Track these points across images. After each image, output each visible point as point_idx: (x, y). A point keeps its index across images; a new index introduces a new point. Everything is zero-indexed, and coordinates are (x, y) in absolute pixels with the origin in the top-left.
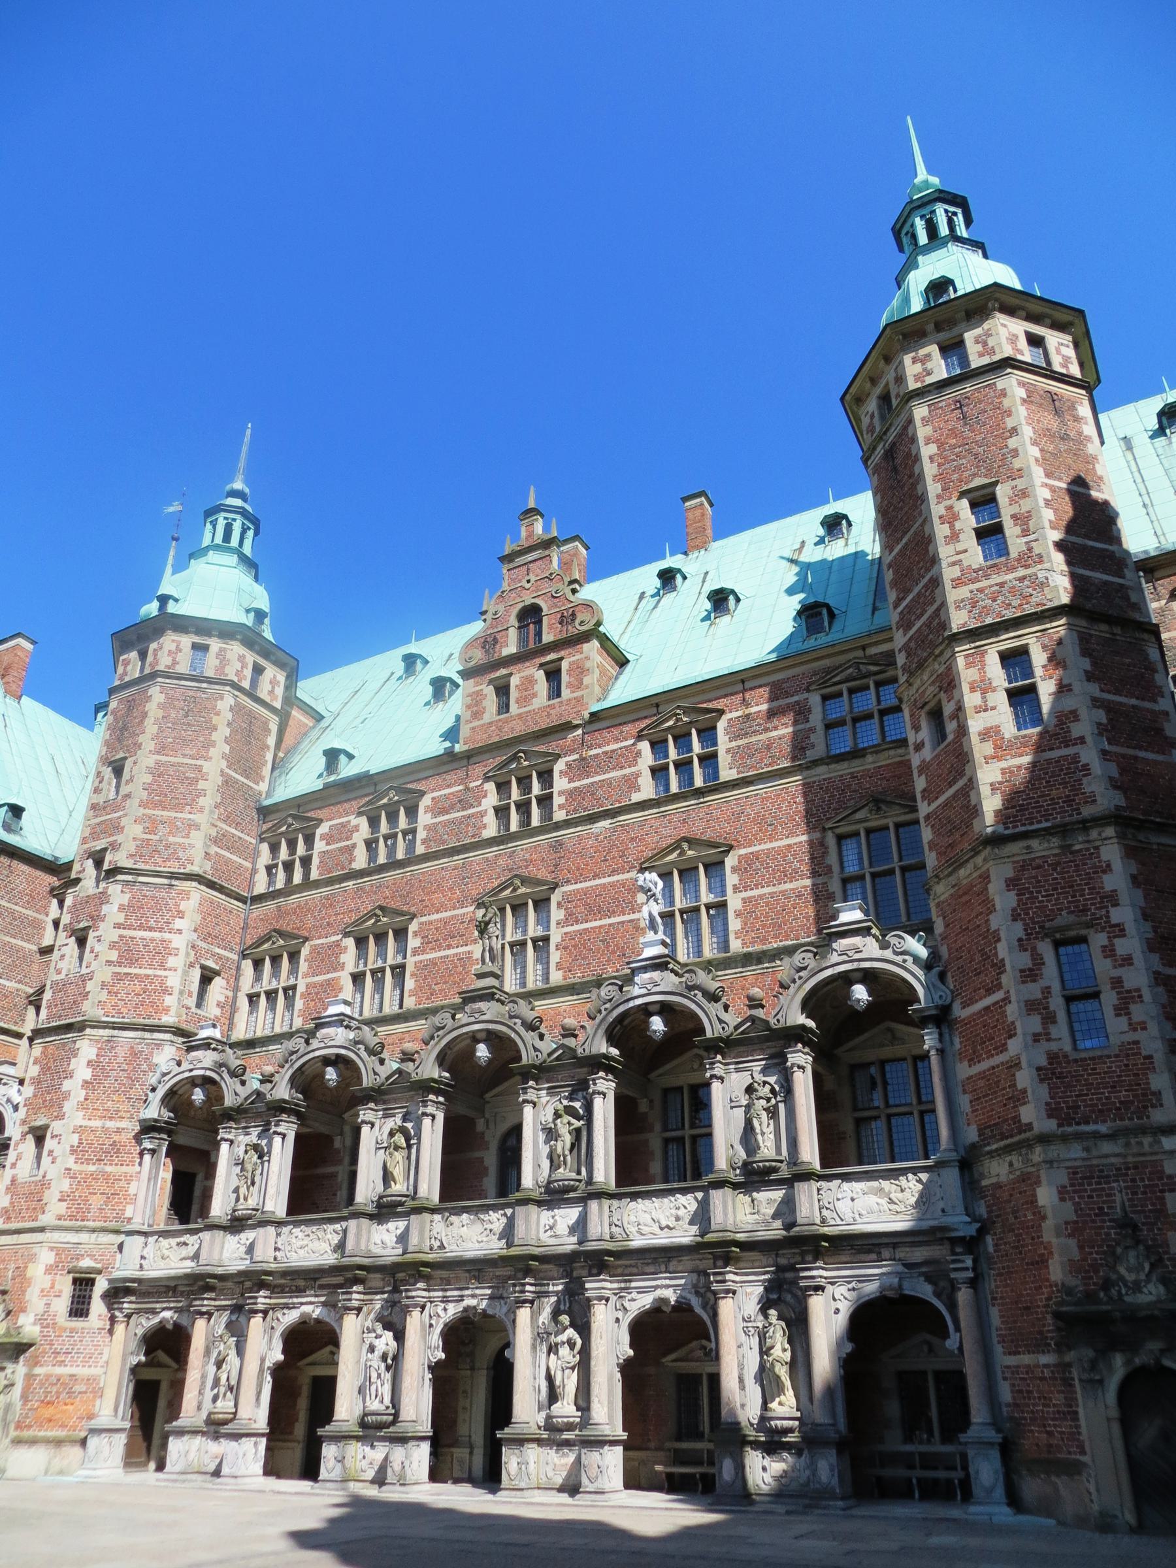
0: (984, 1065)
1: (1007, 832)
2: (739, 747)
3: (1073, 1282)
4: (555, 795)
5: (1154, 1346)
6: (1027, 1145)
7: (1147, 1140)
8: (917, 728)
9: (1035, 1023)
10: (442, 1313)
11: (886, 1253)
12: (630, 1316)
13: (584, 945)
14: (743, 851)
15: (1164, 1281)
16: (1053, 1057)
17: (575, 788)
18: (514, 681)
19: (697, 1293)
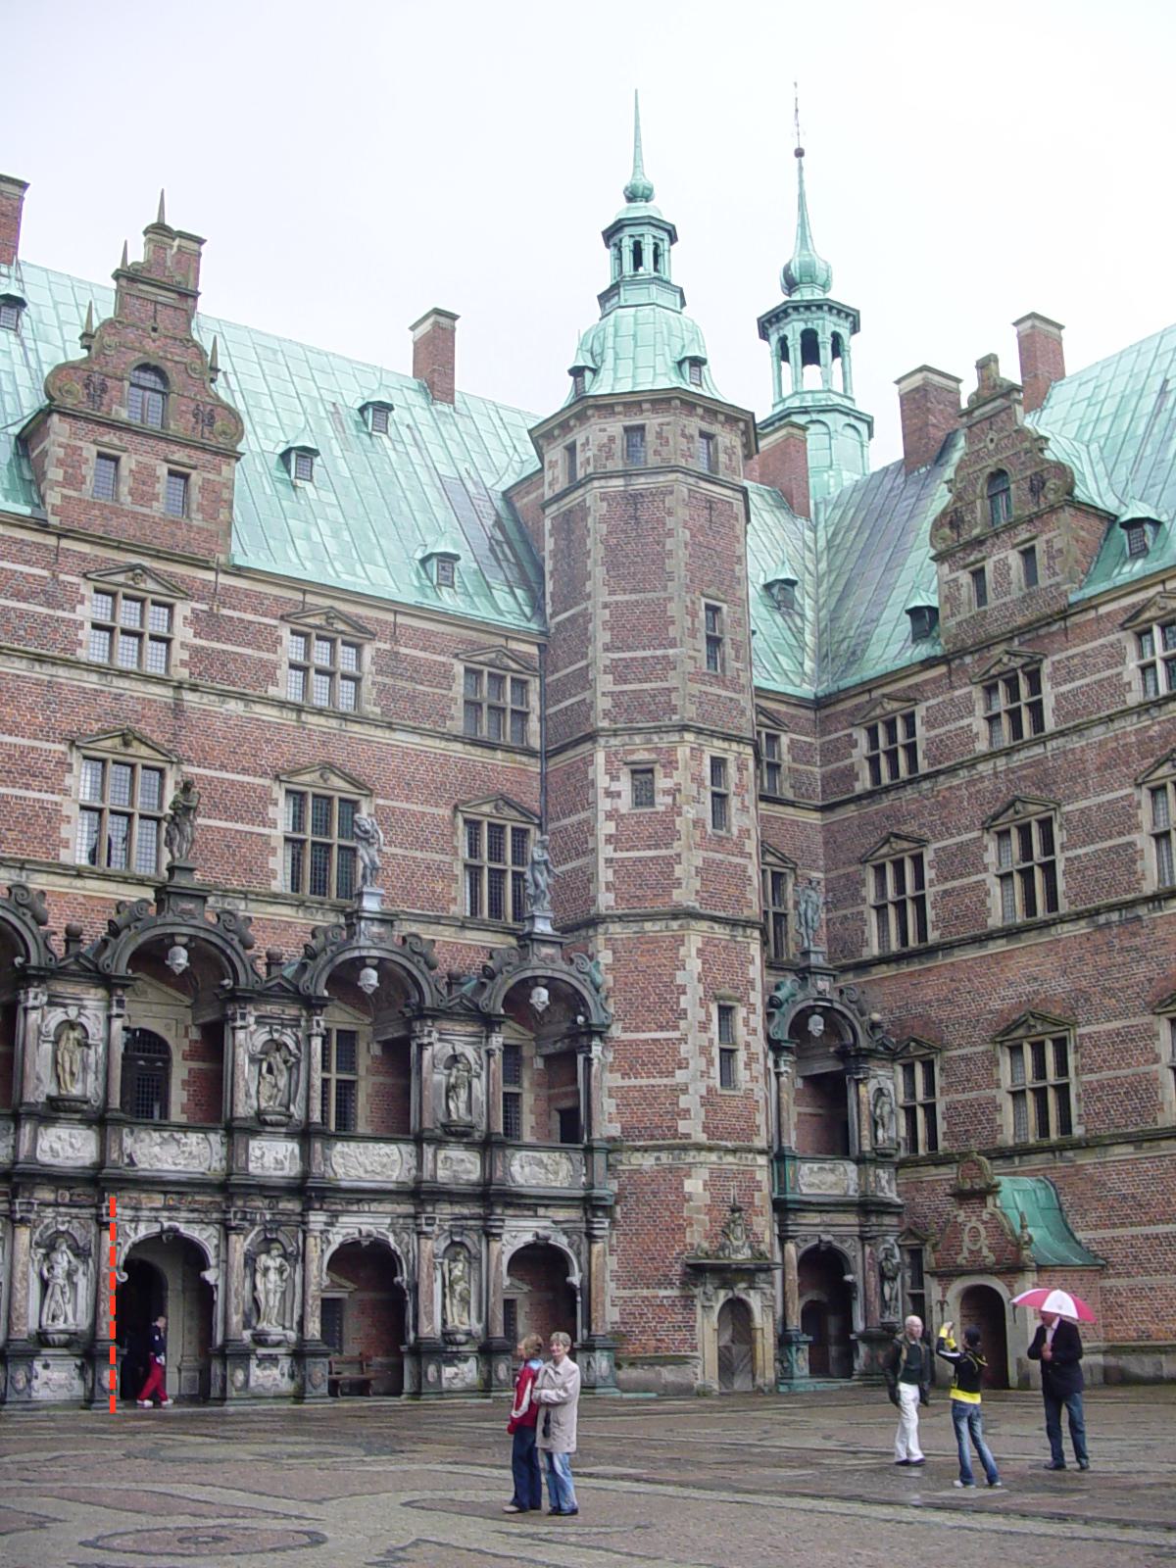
0: (644, 1082)
1: (702, 911)
2: (385, 685)
3: (705, 1245)
4: (175, 645)
5: (743, 1285)
6: (684, 1148)
7: (750, 1156)
8: (614, 778)
9: (702, 1063)
10: (132, 1234)
11: (541, 1211)
12: (334, 1247)
13: (206, 843)
14: (381, 802)
15: (751, 1247)
16: (709, 1090)
17: (203, 648)
18: (128, 463)
19: (394, 1232)
